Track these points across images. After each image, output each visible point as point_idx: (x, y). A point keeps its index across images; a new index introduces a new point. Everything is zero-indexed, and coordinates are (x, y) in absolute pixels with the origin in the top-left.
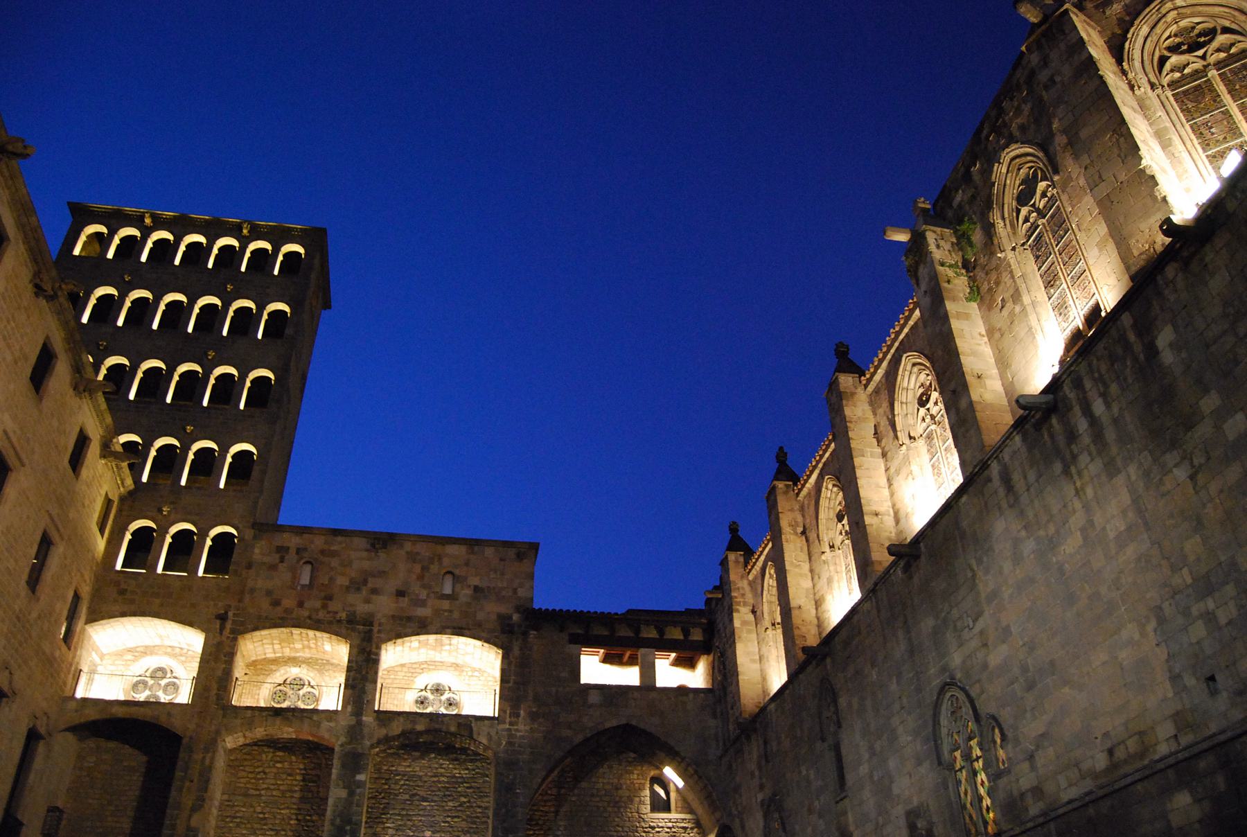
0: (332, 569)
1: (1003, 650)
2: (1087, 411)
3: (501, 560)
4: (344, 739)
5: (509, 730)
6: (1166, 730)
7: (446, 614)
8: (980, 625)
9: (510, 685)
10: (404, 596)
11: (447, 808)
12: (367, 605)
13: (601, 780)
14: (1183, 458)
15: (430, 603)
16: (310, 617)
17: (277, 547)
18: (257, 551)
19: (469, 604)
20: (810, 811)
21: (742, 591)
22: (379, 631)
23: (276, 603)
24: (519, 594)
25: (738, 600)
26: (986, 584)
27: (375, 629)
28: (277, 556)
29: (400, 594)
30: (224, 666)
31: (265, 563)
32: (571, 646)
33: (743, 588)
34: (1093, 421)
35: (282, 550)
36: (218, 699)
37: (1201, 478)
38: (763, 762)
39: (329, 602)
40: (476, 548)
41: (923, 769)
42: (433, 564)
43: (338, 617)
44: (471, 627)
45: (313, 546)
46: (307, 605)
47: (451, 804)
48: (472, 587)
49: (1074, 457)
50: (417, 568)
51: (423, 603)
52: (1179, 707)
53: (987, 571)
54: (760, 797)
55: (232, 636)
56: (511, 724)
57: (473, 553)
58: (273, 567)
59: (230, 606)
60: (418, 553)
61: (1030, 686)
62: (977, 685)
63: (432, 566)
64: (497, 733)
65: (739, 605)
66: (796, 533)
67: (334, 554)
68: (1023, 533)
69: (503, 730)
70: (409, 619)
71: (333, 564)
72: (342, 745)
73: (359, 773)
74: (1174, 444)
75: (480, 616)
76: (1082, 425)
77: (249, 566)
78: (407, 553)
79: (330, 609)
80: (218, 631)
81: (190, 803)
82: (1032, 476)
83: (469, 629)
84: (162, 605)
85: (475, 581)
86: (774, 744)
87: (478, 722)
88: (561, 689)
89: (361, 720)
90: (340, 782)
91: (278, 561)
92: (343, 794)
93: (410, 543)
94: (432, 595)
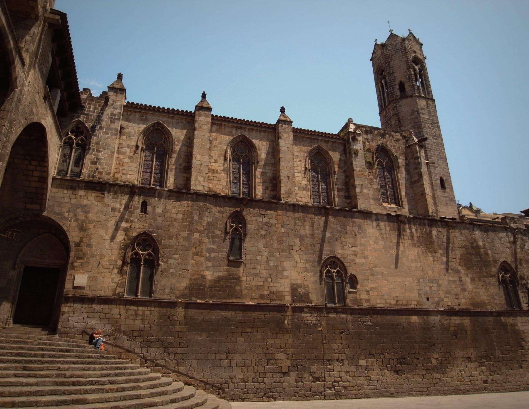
1: (363, 261)
2: (410, 228)
6: (415, 303)
8: (353, 249)
14: (433, 256)
20: (196, 254)
26: (360, 240)
34: (411, 232)
37: (435, 262)
41: (309, 274)
49: (403, 235)
52: (419, 300)
53: (362, 238)
61: (373, 275)
62: (348, 264)
68: (381, 238)
74: (430, 252)
76: (408, 230)
82: (388, 228)
86: (159, 210)
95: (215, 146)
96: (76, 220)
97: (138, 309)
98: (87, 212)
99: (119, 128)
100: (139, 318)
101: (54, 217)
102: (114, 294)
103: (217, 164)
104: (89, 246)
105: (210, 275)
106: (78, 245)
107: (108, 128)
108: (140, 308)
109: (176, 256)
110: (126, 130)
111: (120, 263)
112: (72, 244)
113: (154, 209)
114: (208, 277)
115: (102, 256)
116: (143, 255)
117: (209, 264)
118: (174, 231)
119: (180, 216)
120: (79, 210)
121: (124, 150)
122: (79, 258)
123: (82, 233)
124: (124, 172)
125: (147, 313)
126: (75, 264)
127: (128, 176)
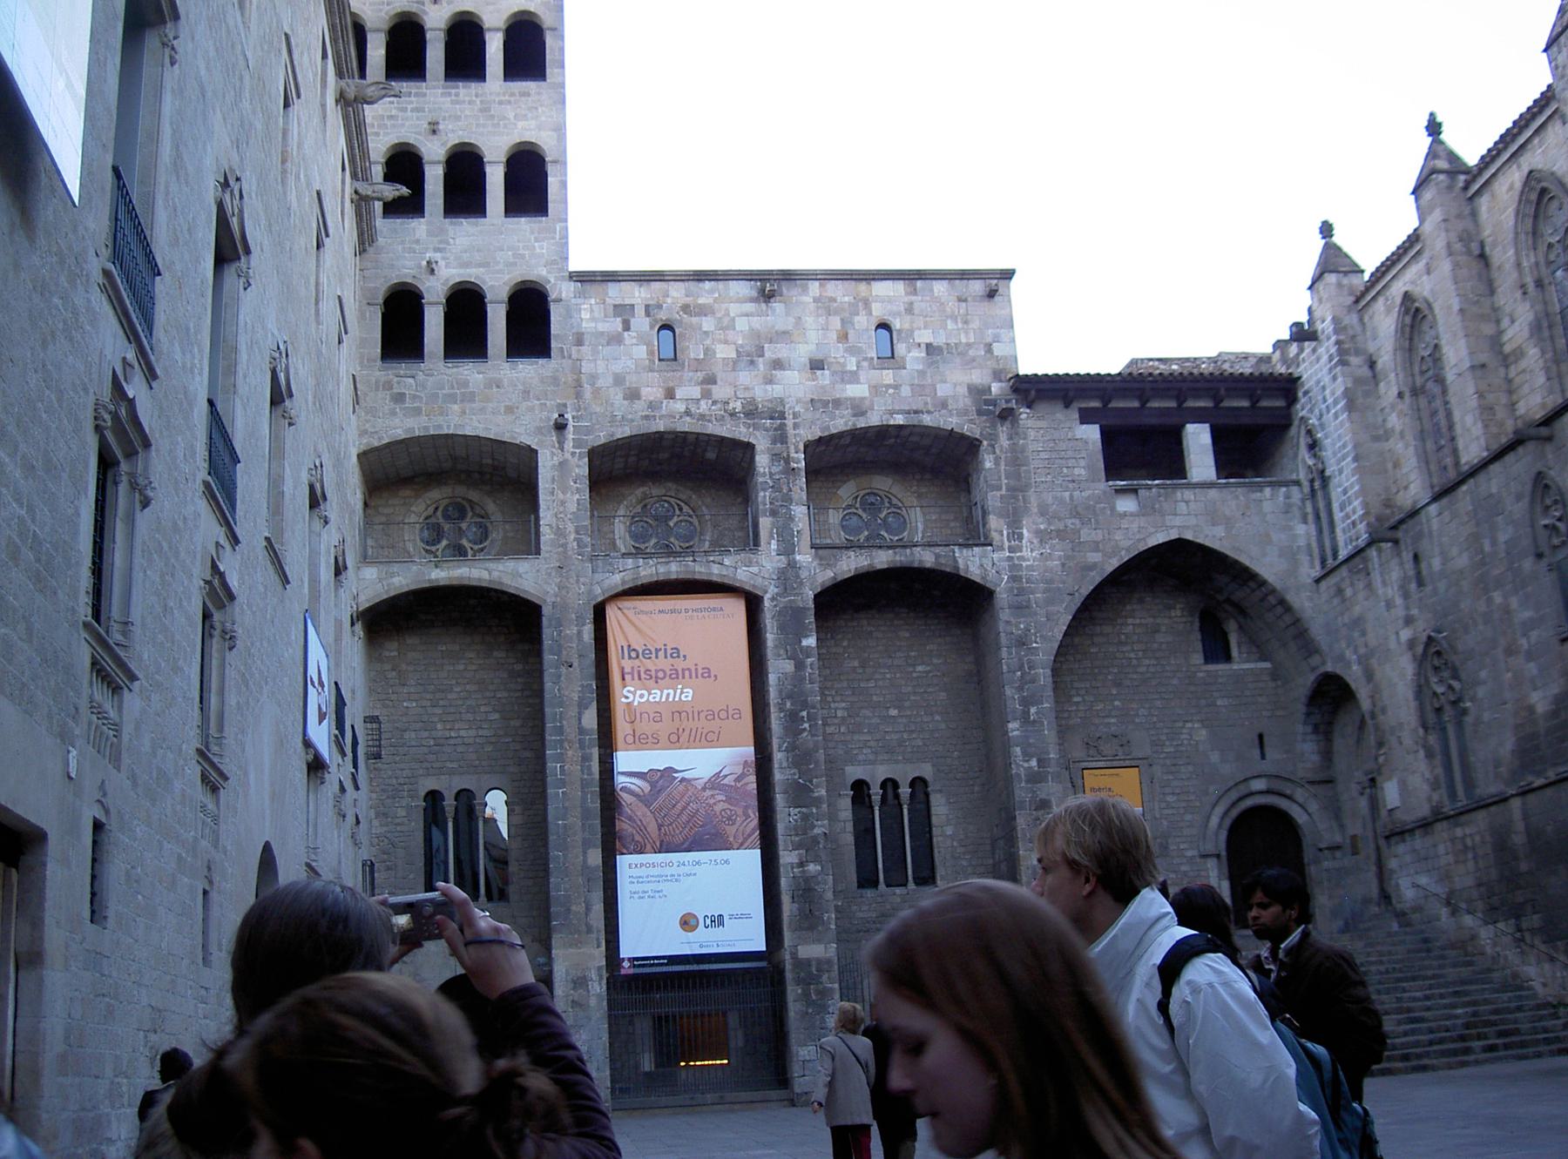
0: (705, 332)
3: (960, 300)
4: (776, 590)
5: (1010, 559)
7: (891, 391)
9: (1003, 492)
10: (823, 369)
11: (915, 675)
12: (769, 387)
13: (1130, 621)
15: (863, 376)
16: (688, 413)
17: (615, 306)
18: (585, 315)
19: (922, 373)
20: (1510, 651)
21: (1351, 332)
22: (796, 426)
23: (633, 395)
24: (996, 354)
25: (1346, 346)
27: (790, 422)
28: (619, 319)
29: (816, 365)
30: (577, 496)
31: (602, 333)
32: (1084, 426)
33: (1352, 327)
35: (623, 312)
36: (578, 545)
38: (1413, 586)
39: (714, 388)
40: (919, 283)
42: (858, 314)
43: (731, 406)
44: (930, 407)
45: (669, 300)
46: (679, 393)
47: (920, 668)
48: (924, 347)
50: (836, 322)
51: (853, 378)
54: (1405, 634)
55: (578, 451)
56: (1011, 550)
57: (915, 292)
58: (616, 339)
59: (565, 405)
60: (833, 300)
63: (857, 319)
64: (993, 564)
65: (1350, 355)
66: (1469, 252)
67: (703, 311)
69: (1000, 560)
70: (837, 403)
71: (705, 329)
72: (773, 599)
73: (807, 637)
75: (943, 390)
77: (579, 341)
78: (816, 300)
79: (715, 396)
80: (557, 445)
81: (575, 697)
83: (929, 412)
84: (464, 412)
85: (925, 336)
86: (1436, 563)
87: (965, 551)
88: (1076, 493)
89: (794, 559)
90: (782, 652)
91: (620, 330)
92: (789, 666)
93: (817, 283)
94: (865, 364)
95: (1499, 267)
96: (1359, 663)
97: (1466, 835)
98: (1364, 634)
99: (1365, 372)
100: (1470, 855)
101: (1338, 669)
102: (1432, 811)
103: (1517, 323)
104: (1384, 710)
105: (1540, 701)
106: (1373, 716)
107: (1336, 403)
108: (1468, 831)
109: (1483, 674)
110: (1379, 365)
111: (1421, 731)
112: (1367, 717)
113: (1430, 566)
114: (1541, 708)
115: (1401, 724)
116: (1443, 694)
117: (1532, 669)
118: (1465, 605)
119: (1462, 561)
120: (1356, 634)
121: (1389, 425)
122: (1380, 744)
123: (1371, 686)
124: (1405, 484)
125: (1477, 838)
126: (1381, 759)
127: (1412, 486)
